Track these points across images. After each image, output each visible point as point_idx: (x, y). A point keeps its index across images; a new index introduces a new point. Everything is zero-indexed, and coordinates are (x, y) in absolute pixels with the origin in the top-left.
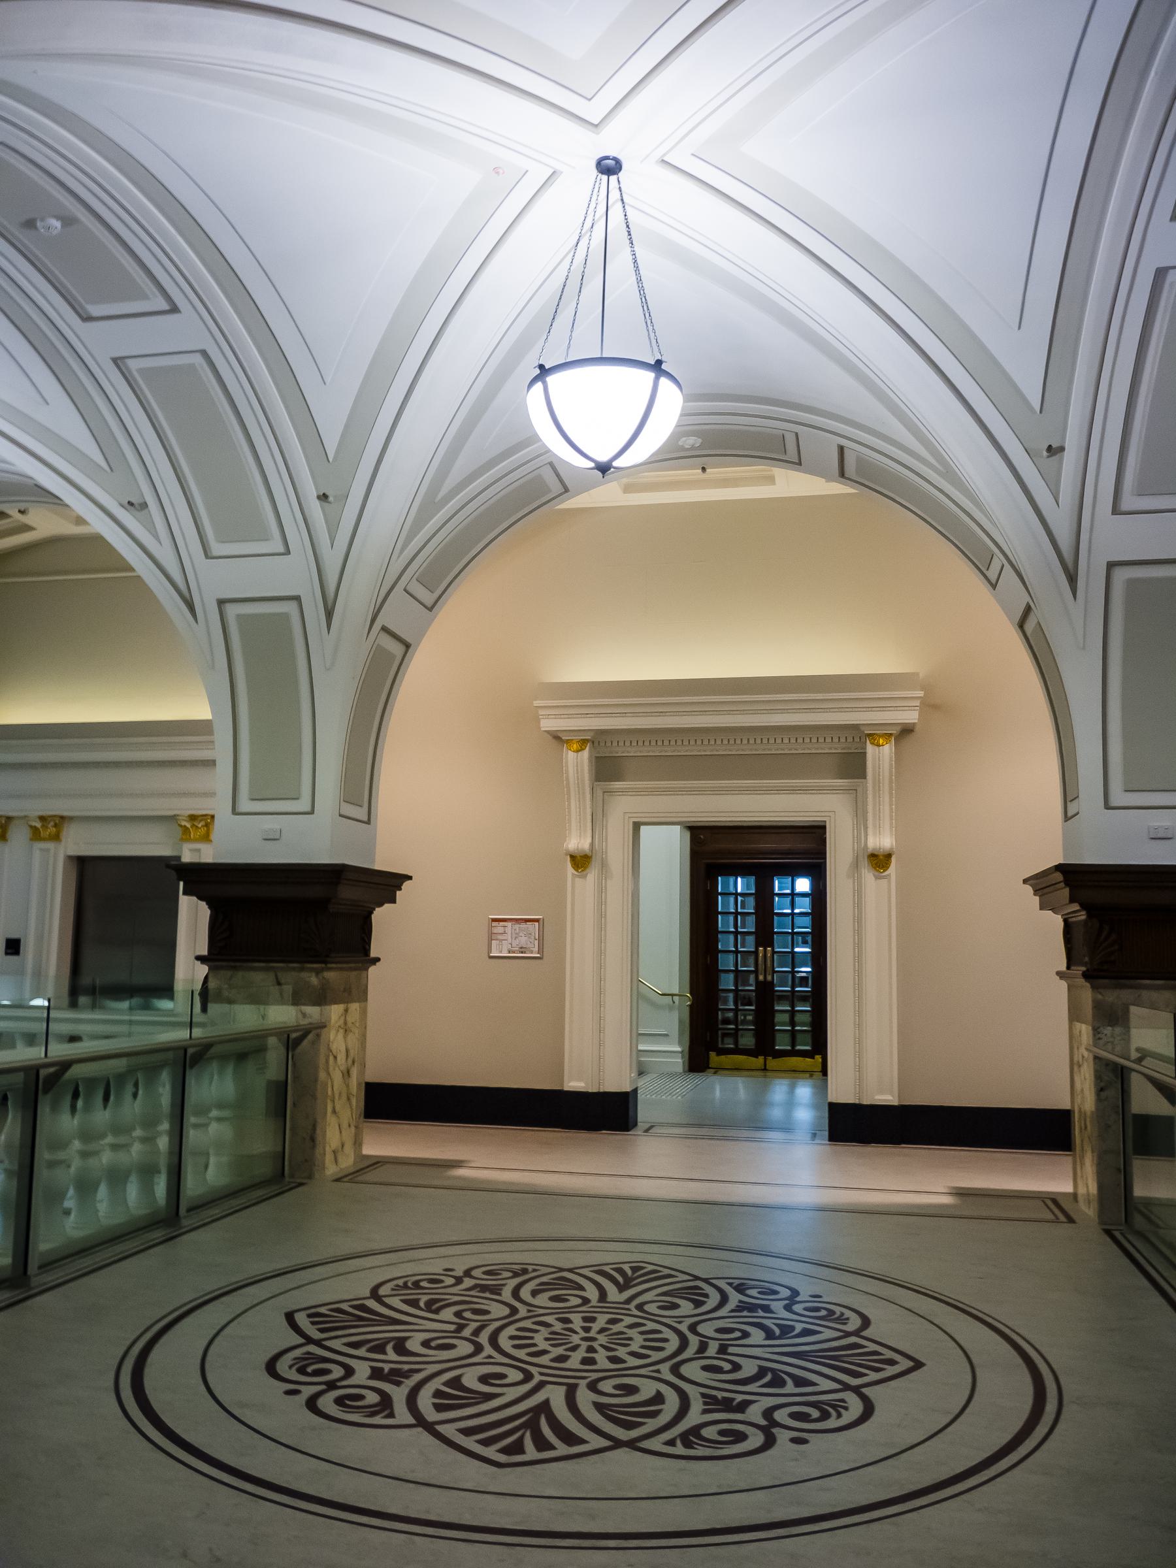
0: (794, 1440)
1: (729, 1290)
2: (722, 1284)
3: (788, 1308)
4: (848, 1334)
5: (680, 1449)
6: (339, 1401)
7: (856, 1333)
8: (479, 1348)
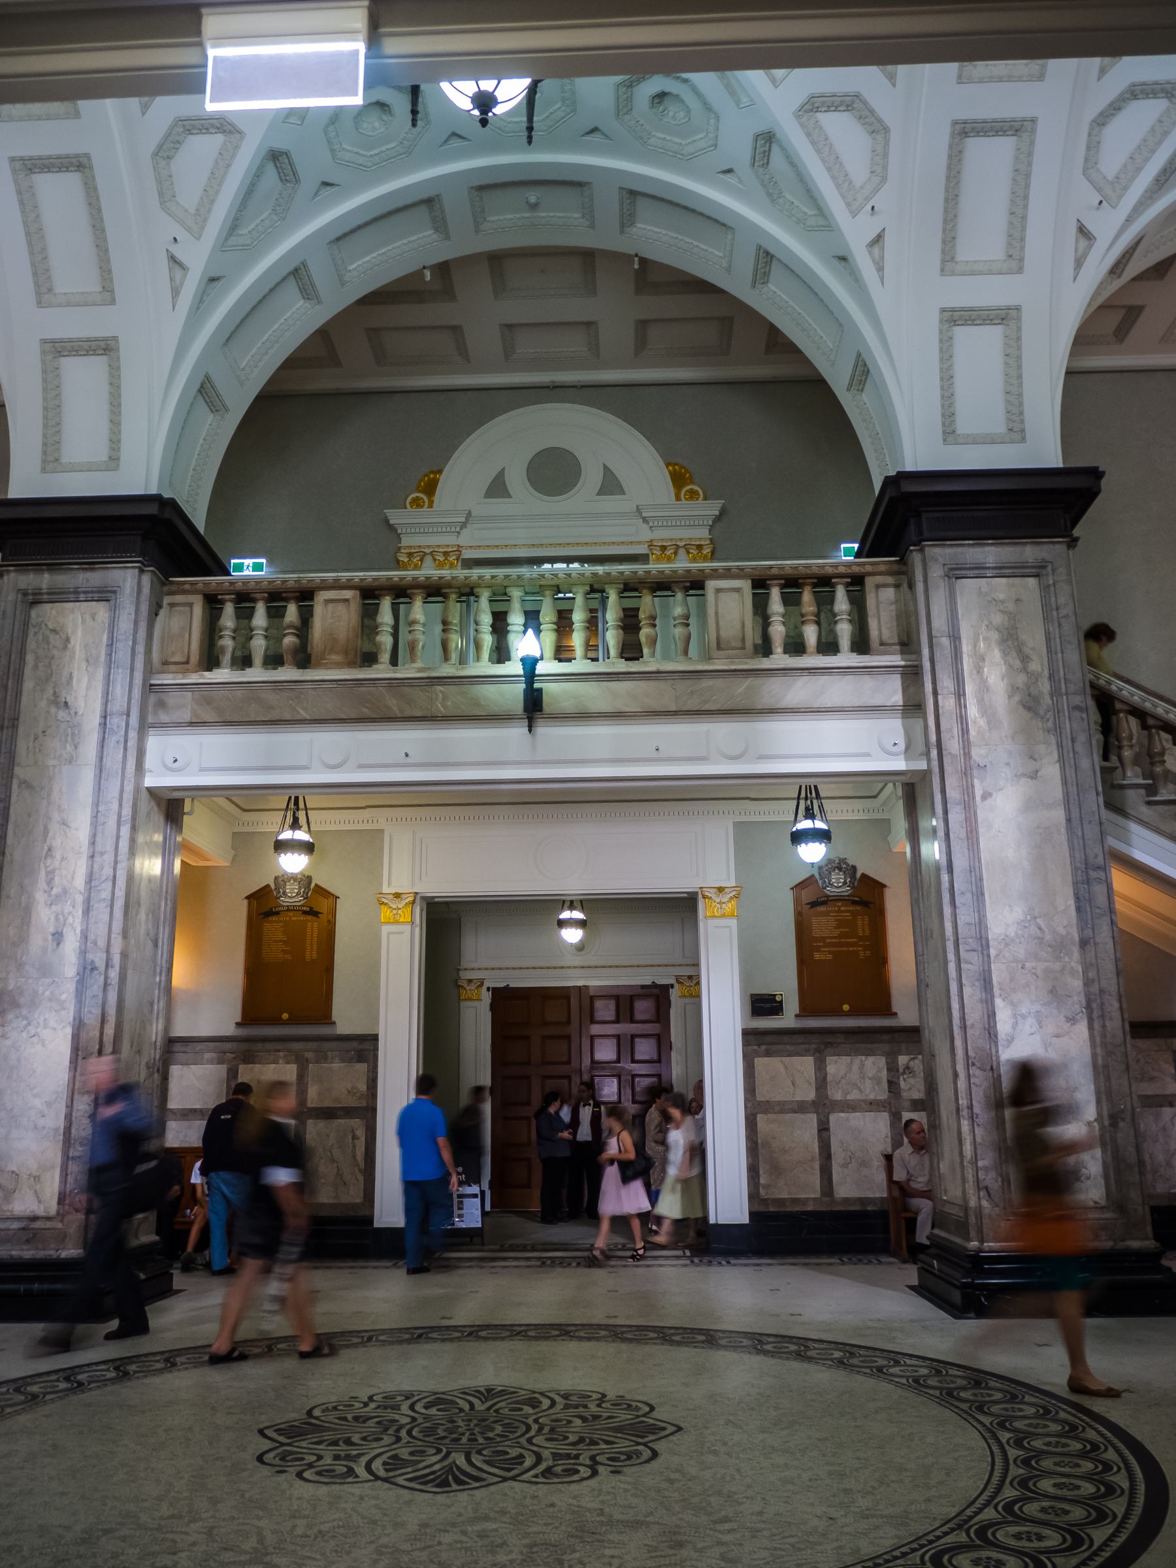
0: (612, 1472)
1: (557, 1398)
2: (552, 1395)
3: (599, 1406)
4: (638, 1417)
5: (541, 1480)
6: (319, 1473)
7: (644, 1415)
8: (398, 1439)
